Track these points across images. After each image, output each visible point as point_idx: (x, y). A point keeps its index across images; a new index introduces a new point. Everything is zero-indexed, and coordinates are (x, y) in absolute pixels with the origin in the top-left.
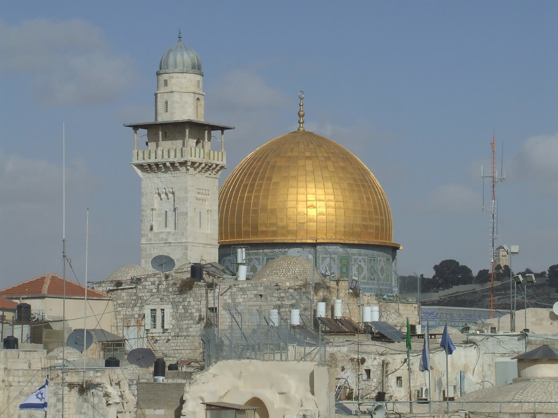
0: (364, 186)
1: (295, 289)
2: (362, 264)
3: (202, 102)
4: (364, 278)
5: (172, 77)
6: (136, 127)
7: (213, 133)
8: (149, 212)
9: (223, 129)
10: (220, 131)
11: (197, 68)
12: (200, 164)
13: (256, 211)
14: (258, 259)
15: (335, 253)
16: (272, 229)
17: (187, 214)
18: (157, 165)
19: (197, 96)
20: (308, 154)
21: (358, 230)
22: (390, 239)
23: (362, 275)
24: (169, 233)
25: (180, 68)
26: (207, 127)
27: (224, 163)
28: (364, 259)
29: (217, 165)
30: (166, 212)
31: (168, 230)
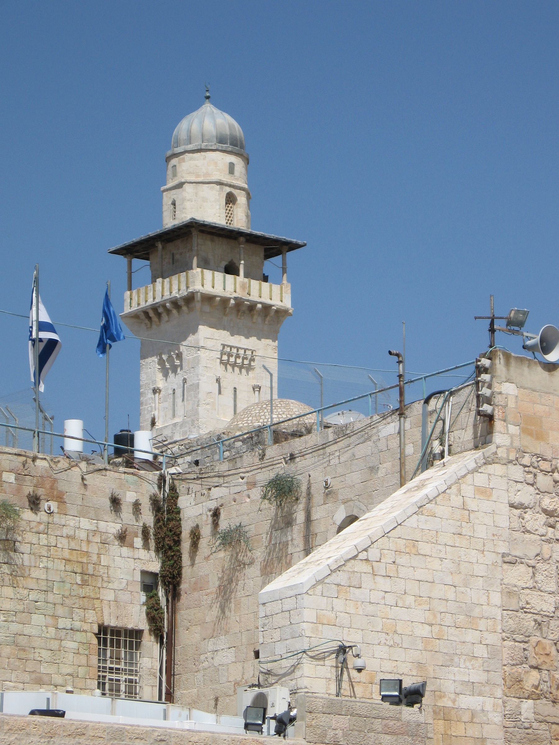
1: (243, 441)
3: (242, 199)
5: (184, 160)
8: (150, 395)
11: (231, 144)
12: (225, 301)
17: (198, 385)
18: (154, 308)
19: (228, 189)
24: (175, 425)
26: (242, 239)
27: (287, 303)
29: (267, 308)
30: (174, 390)
31: (177, 420)
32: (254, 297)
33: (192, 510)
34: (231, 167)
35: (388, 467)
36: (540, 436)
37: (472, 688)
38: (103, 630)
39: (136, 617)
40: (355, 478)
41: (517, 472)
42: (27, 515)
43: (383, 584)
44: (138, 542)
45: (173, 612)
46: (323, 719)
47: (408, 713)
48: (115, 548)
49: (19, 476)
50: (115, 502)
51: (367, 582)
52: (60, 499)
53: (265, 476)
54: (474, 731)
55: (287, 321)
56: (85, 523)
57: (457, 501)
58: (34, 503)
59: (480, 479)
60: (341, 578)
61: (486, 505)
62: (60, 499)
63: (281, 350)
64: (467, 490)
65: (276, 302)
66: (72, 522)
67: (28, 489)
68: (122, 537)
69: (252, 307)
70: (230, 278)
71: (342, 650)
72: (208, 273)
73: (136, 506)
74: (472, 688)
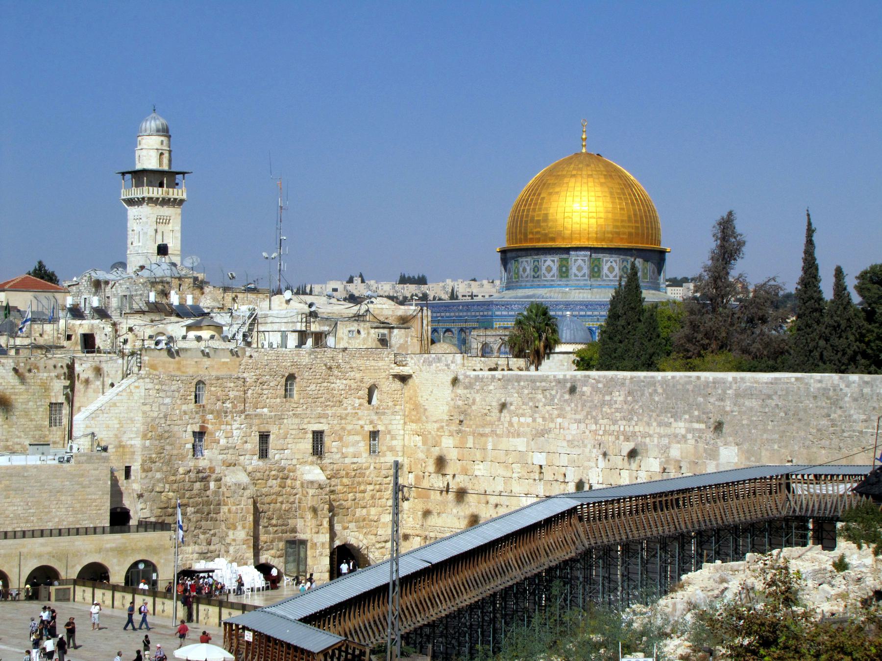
0: (620, 198)
2: (614, 264)
4: (615, 276)
6: (123, 174)
7: (177, 176)
9: (184, 173)
10: (181, 176)
12: (158, 199)
13: (526, 222)
14: (527, 262)
15: (585, 256)
16: (537, 236)
20: (574, 172)
21: (610, 236)
22: (659, 243)
23: (614, 274)
25: (148, 132)
27: (185, 197)
28: (615, 261)
29: (175, 199)
31: (140, 244)
32: (171, 196)
33: (78, 368)
34: (162, 142)
35: (120, 372)
36: (155, 369)
37: (131, 439)
38: (51, 404)
39: (61, 399)
40: (113, 372)
41: (147, 380)
42: (27, 374)
43: (105, 415)
44: (62, 377)
45: (73, 396)
46: (79, 458)
47: (104, 454)
48: (55, 381)
49: (25, 364)
50: (55, 367)
51: (101, 415)
52: (38, 368)
53: (94, 364)
54: (132, 450)
55: (184, 204)
56: (45, 374)
57: (128, 391)
58: (30, 371)
59: (136, 384)
60: (93, 415)
61: (137, 390)
62: (38, 368)
63: (183, 215)
64: (132, 387)
65: (180, 197)
66: (41, 374)
67: (28, 367)
68: (58, 377)
69: (169, 199)
70: (160, 189)
71: (93, 434)
72: (151, 189)
73: (62, 367)
74: (131, 439)
